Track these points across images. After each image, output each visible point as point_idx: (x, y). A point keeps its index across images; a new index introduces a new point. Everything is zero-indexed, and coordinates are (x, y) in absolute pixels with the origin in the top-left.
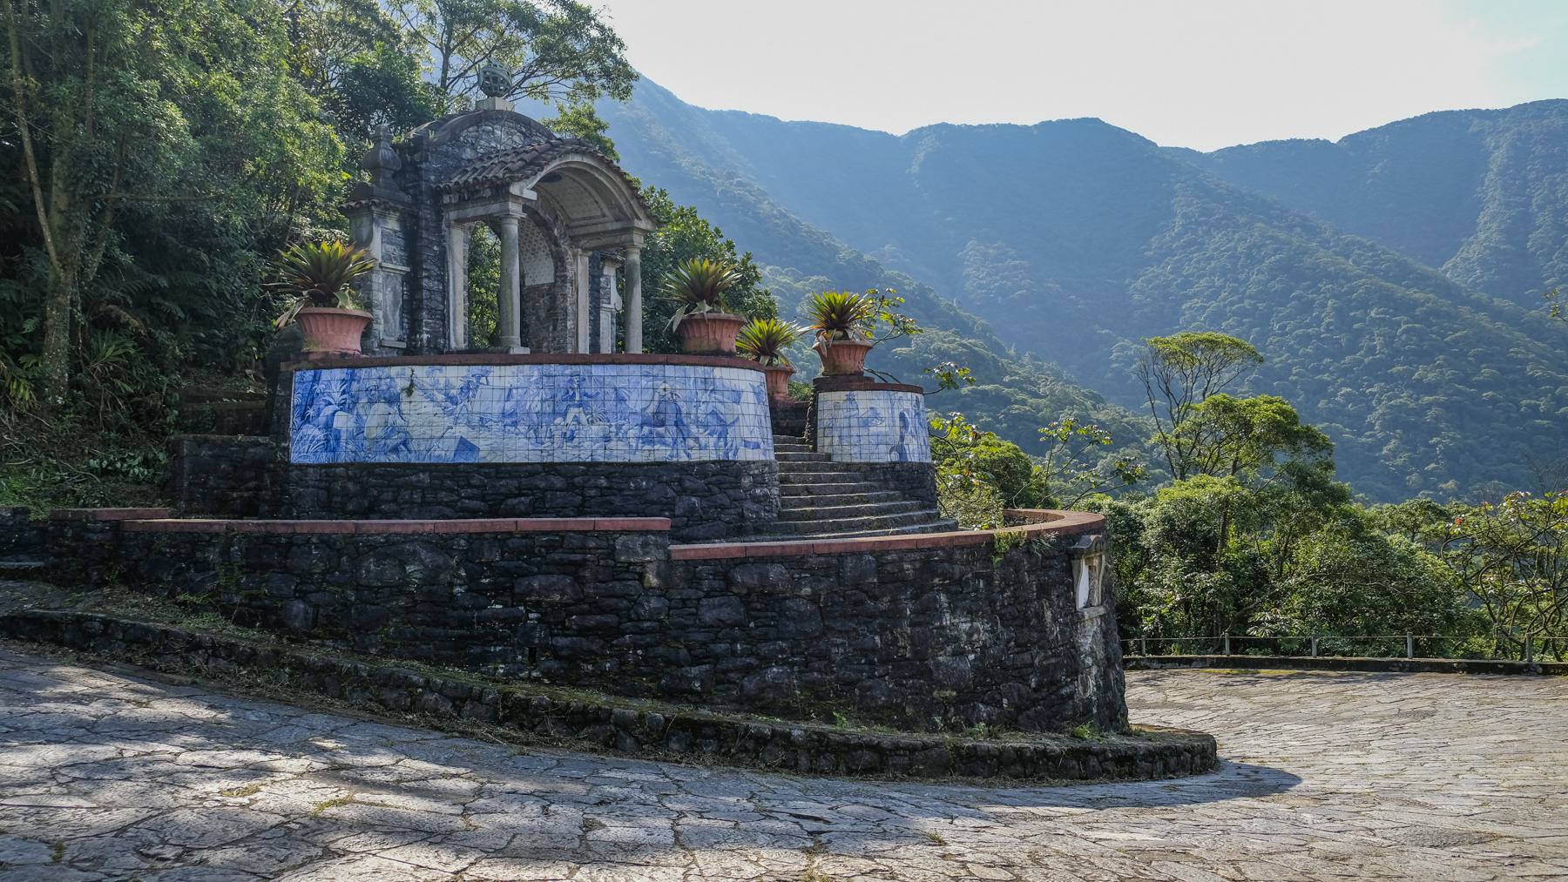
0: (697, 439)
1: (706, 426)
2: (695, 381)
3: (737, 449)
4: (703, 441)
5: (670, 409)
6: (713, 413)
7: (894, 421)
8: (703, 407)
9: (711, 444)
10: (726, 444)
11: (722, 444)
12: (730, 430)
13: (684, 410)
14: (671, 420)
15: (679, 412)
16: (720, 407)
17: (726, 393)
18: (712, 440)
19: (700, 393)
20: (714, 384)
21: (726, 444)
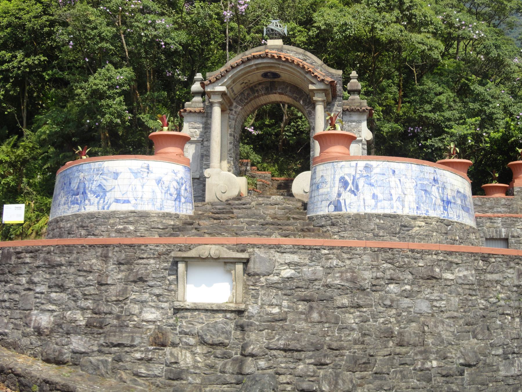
0: (89, 200)
1: (94, 193)
2: (94, 170)
3: (110, 204)
4: (92, 201)
5: (82, 186)
6: (100, 186)
7: (334, 184)
8: (95, 183)
9: (96, 202)
10: (104, 202)
11: (102, 201)
12: (108, 194)
13: (87, 186)
14: (81, 190)
15: (84, 188)
16: (104, 181)
17: (109, 174)
18: (97, 200)
19: (95, 176)
20: (103, 170)
21: (104, 202)
